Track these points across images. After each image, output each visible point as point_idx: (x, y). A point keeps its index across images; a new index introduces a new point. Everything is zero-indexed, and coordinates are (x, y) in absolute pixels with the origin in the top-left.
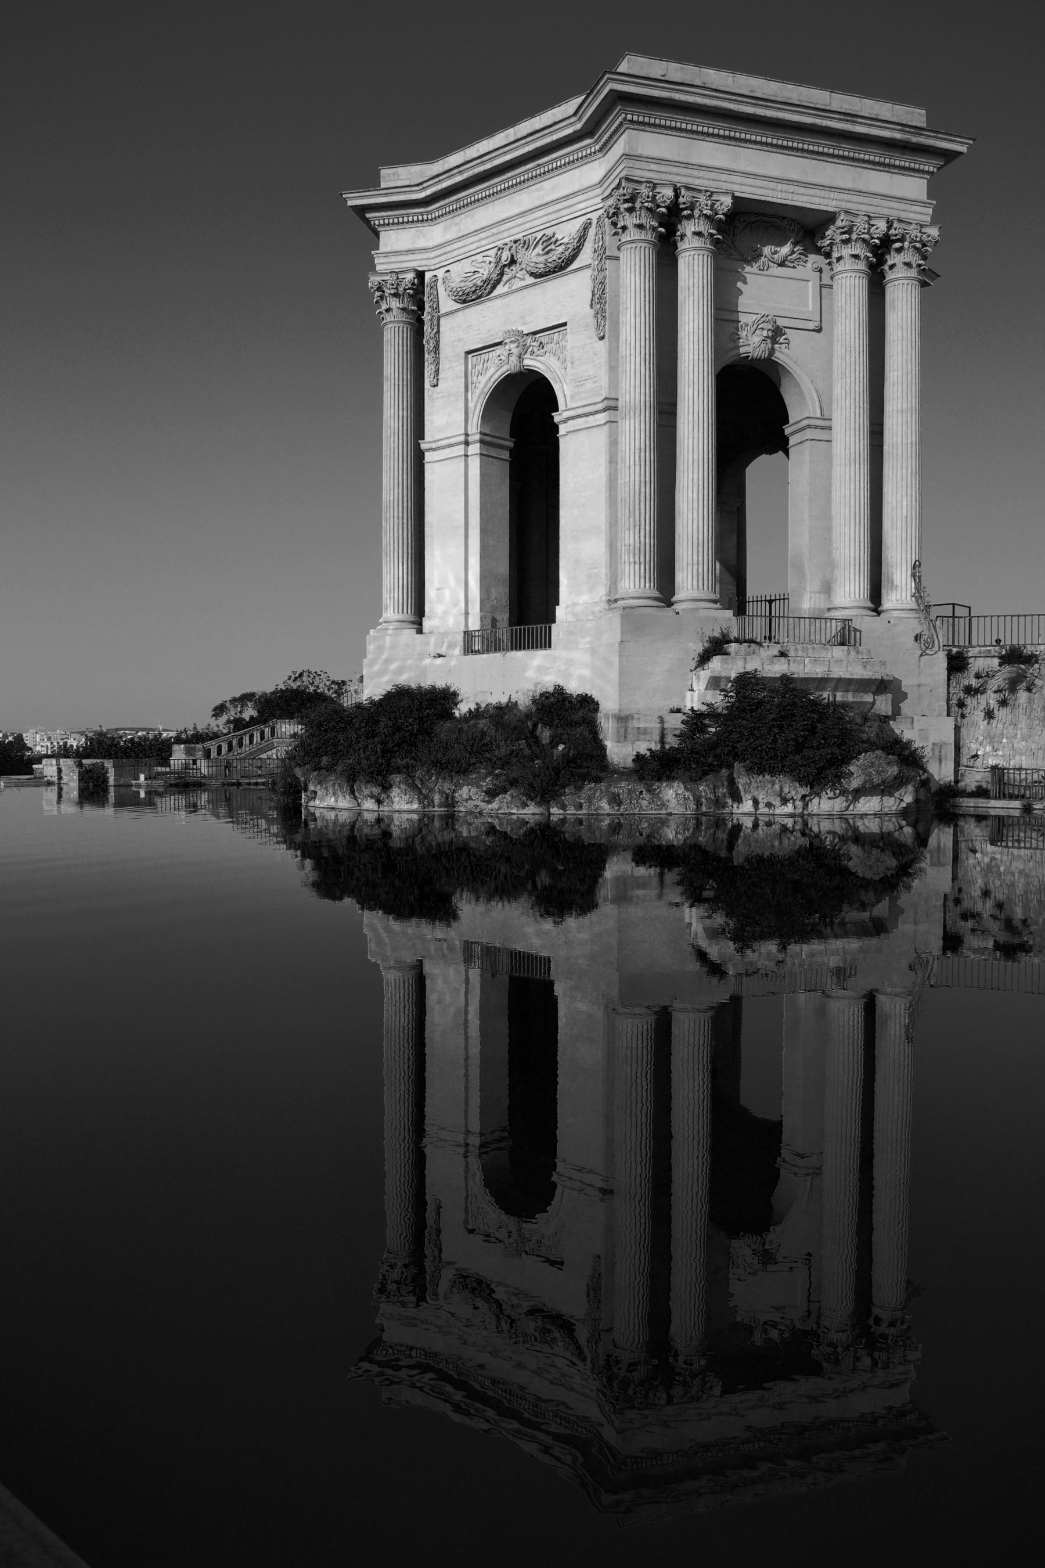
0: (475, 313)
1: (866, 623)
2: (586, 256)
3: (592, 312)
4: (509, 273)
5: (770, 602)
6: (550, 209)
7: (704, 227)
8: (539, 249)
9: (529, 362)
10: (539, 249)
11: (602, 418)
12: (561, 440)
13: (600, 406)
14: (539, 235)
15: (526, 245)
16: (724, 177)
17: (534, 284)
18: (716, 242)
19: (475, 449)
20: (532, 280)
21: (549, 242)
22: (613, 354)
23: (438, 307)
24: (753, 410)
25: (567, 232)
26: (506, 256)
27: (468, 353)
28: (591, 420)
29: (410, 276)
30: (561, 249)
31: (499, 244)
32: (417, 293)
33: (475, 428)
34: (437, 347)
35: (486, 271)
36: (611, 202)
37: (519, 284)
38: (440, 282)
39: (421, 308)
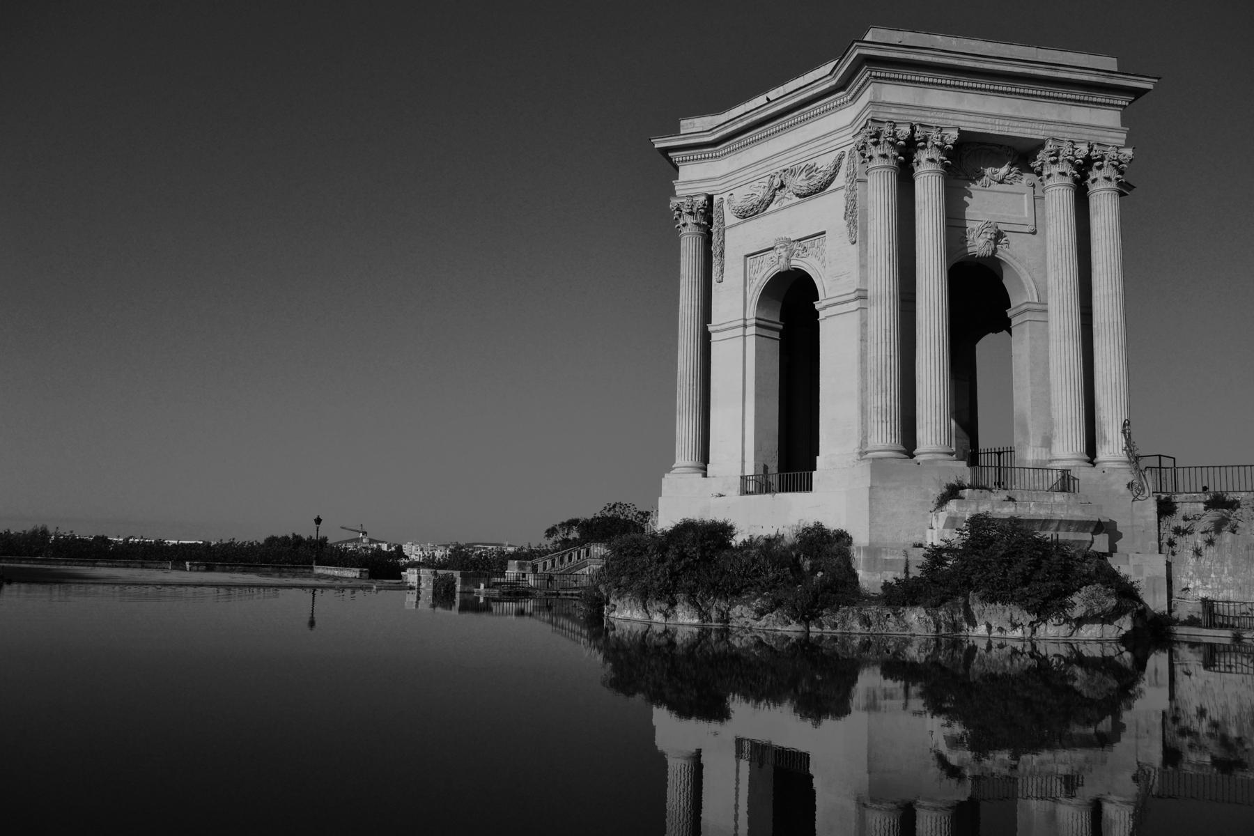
0: (753, 225)
1: (1083, 473)
2: (840, 180)
3: (846, 223)
4: (779, 194)
5: (999, 454)
6: (812, 145)
7: (936, 155)
8: (803, 176)
9: (796, 263)
10: (803, 176)
11: (855, 305)
12: (821, 324)
13: (852, 296)
14: (803, 165)
15: (793, 172)
16: (951, 116)
17: (799, 203)
18: (945, 166)
19: (752, 330)
20: (798, 199)
21: (811, 170)
22: (863, 254)
23: (723, 222)
24: (980, 298)
25: (825, 163)
26: (777, 182)
27: (747, 256)
28: (845, 307)
29: (702, 199)
30: (820, 175)
31: (772, 173)
32: (708, 210)
33: (752, 313)
34: (722, 252)
35: (761, 193)
36: (860, 138)
37: (786, 202)
38: (725, 204)
39: (711, 223)
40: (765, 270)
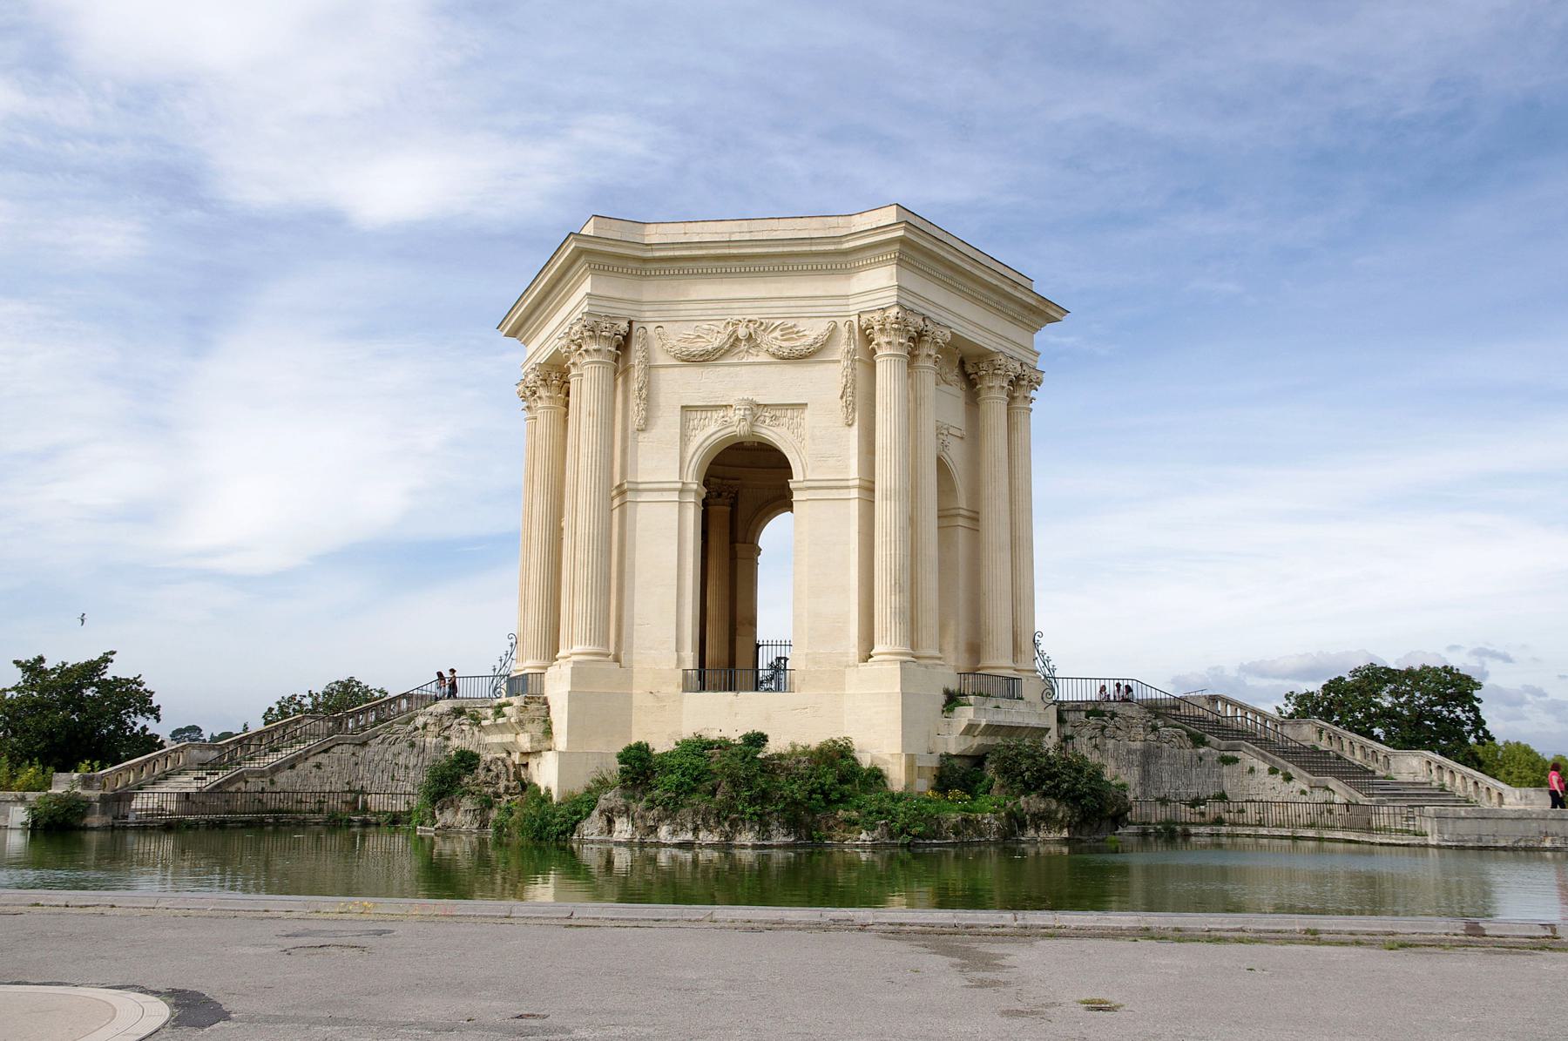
0: (692, 372)
3: (842, 403)
6: (792, 303)
10: (777, 333)
19: (691, 498)
20: (764, 357)
21: (789, 333)
26: (742, 332)
29: (624, 325)
40: (709, 433)
